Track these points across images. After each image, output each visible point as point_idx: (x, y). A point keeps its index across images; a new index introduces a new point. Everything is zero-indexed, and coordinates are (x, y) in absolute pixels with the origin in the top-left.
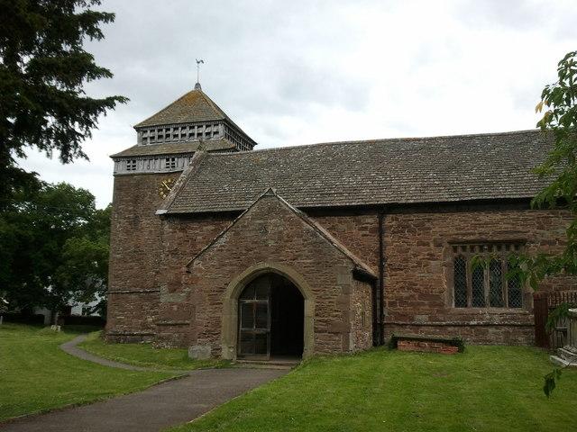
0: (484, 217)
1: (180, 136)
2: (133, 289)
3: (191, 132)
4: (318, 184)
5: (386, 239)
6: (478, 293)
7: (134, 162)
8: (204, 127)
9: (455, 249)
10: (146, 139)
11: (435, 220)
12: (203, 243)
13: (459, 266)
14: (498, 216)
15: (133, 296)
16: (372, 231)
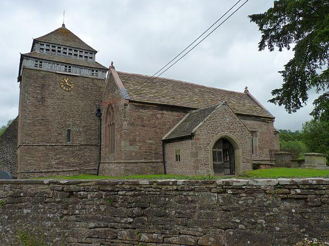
15: (41, 148)
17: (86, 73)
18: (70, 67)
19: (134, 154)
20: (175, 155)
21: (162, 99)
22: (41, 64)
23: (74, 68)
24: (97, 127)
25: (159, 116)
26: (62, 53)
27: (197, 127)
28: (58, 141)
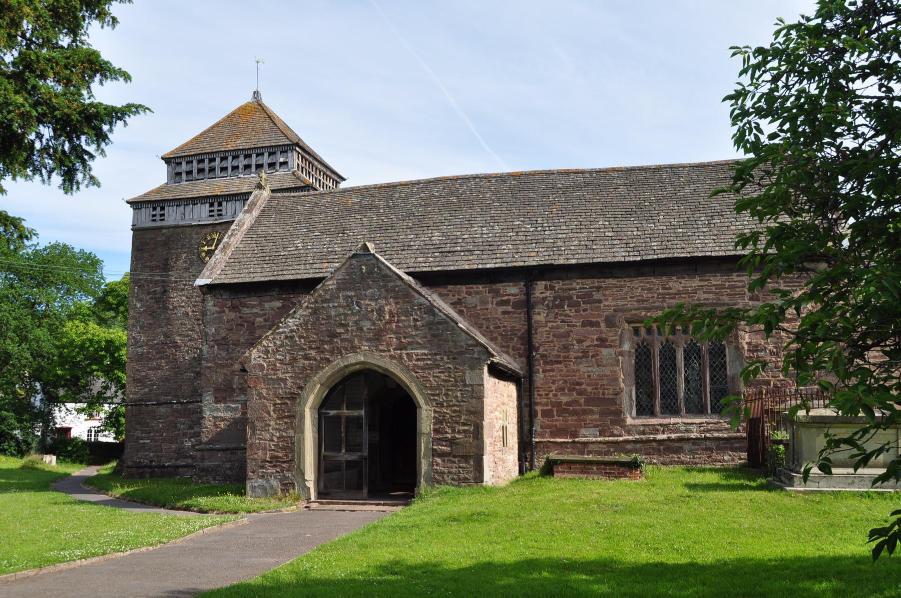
0: (676, 284)
1: (230, 169)
2: (163, 398)
3: (246, 162)
4: (437, 237)
5: (536, 318)
6: (670, 395)
7: (163, 209)
8: (266, 155)
9: (636, 331)
10: (179, 174)
11: (606, 289)
12: (264, 327)
13: (643, 356)
14: (696, 282)
16: (516, 305)
22: (162, 212)
23: (229, 204)
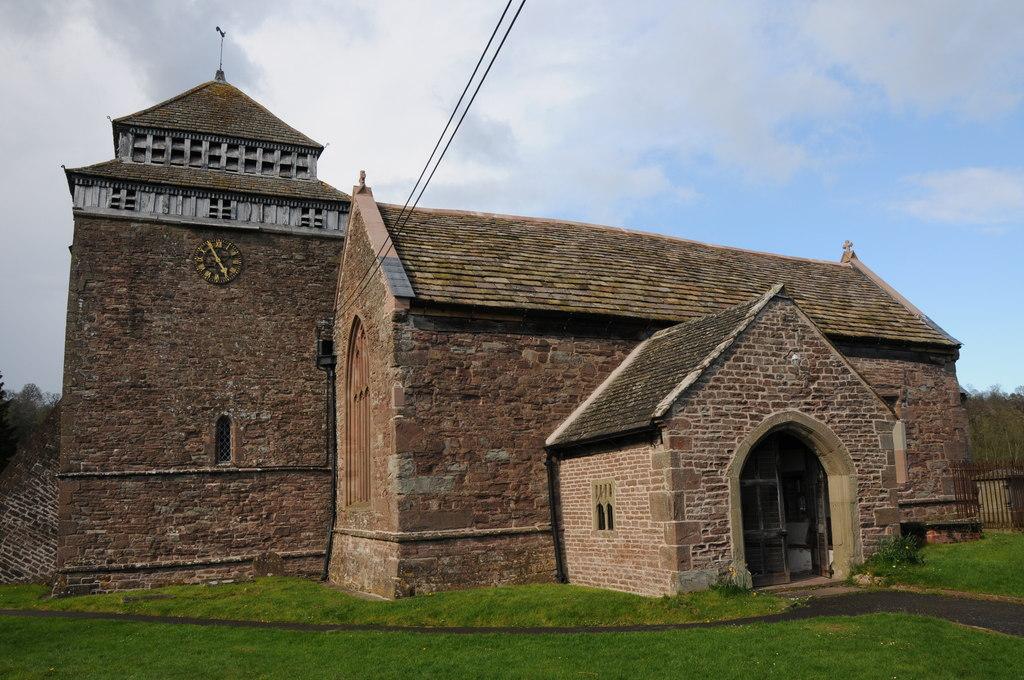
7: (131, 193)
15: (129, 484)
17: (280, 218)
18: (227, 203)
19: (434, 505)
20: (592, 505)
21: (543, 293)
23: (241, 206)
24: (321, 406)
25: (528, 355)
26: (204, 160)
27: (675, 393)
28: (187, 456)
